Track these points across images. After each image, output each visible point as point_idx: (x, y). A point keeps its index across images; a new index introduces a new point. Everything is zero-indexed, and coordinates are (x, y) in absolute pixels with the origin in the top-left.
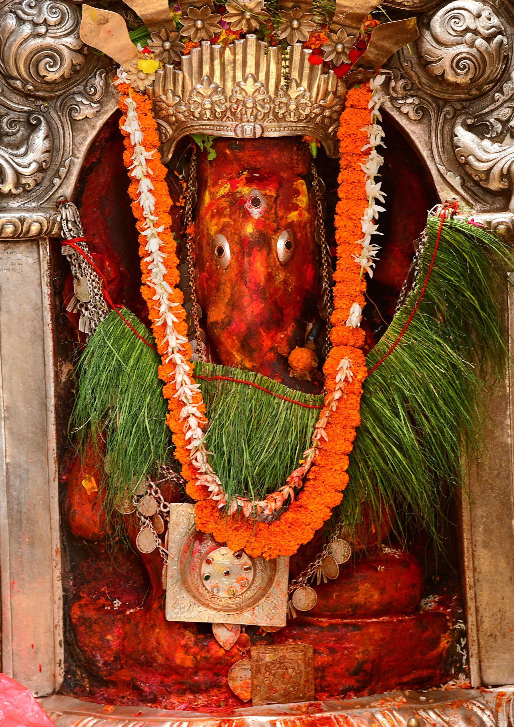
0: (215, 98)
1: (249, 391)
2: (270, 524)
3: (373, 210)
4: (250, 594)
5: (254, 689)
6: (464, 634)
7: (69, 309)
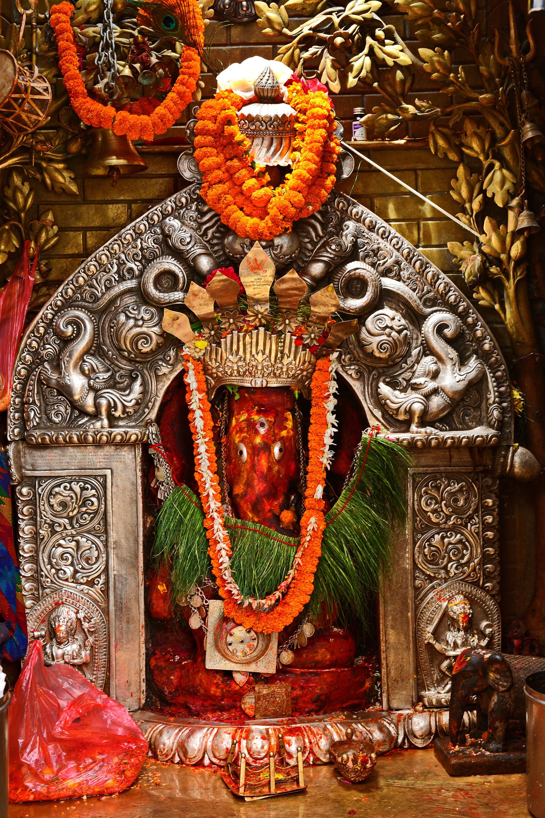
0: (240, 364)
1: (257, 535)
2: (267, 613)
3: (331, 431)
4: (255, 654)
5: (256, 710)
6: (379, 679)
7: (152, 485)
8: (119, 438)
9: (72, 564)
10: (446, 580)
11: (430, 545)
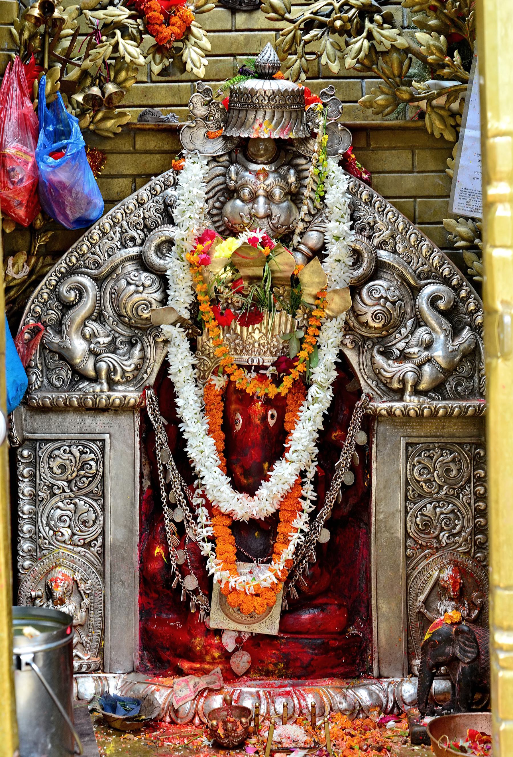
8: (118, 401)
9: (69, 527)
10: (438, 550)
11: (422, 514)
